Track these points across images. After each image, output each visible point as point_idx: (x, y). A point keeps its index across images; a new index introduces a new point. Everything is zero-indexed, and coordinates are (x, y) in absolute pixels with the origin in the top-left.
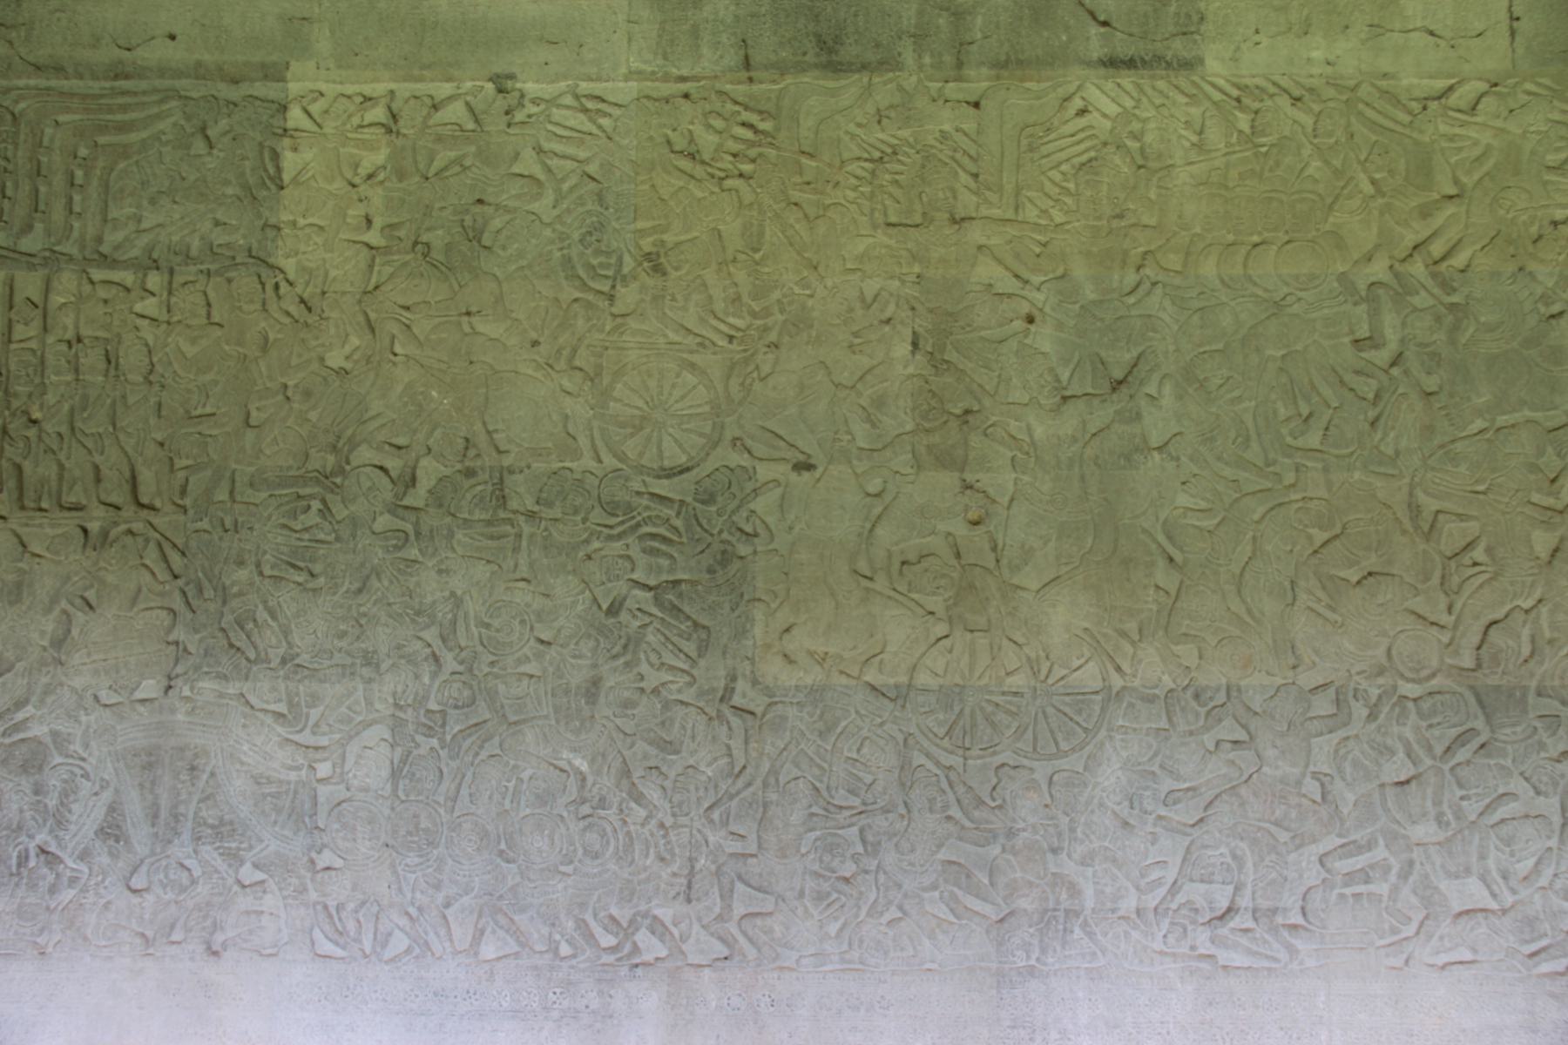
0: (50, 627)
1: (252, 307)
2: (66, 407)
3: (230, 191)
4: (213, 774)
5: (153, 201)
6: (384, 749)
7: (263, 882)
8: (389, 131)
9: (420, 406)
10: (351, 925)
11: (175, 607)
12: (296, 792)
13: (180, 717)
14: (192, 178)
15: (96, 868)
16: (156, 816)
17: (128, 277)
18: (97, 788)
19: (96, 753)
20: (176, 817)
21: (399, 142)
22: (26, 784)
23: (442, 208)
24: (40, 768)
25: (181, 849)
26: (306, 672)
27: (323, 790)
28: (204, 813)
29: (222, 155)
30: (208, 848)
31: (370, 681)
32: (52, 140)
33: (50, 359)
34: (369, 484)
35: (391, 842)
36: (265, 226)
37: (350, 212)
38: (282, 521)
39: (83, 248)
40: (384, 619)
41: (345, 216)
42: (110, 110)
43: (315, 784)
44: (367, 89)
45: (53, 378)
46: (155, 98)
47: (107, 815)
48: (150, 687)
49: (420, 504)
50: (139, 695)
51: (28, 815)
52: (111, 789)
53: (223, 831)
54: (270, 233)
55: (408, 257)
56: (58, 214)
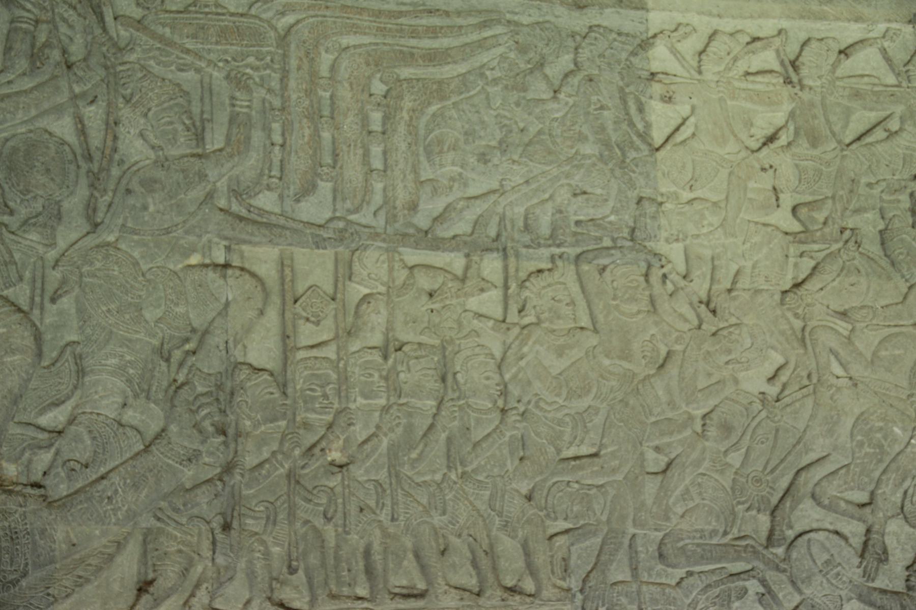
1: (634, 308)
3: (589, 149)
5: (483, 158)
8: (788, 81)
9: (881, 447)
14: (533, 130)
17: (457, 262)
21: (806, 96)
23: (870, 185)
29: (571, 101)
32: (333, 68)
33: (356, 373)
34: (826, 557)
36: (640, 200)
37: (752, 184)
39: (392, 219)
41: (746, 189)
42: (414, 33)
44: (752, 27)
45: (361, 401)
46: (472, 20)
49: (900, 586)
54: (650, 209)
55: (835, 247)
56: (353, 171)
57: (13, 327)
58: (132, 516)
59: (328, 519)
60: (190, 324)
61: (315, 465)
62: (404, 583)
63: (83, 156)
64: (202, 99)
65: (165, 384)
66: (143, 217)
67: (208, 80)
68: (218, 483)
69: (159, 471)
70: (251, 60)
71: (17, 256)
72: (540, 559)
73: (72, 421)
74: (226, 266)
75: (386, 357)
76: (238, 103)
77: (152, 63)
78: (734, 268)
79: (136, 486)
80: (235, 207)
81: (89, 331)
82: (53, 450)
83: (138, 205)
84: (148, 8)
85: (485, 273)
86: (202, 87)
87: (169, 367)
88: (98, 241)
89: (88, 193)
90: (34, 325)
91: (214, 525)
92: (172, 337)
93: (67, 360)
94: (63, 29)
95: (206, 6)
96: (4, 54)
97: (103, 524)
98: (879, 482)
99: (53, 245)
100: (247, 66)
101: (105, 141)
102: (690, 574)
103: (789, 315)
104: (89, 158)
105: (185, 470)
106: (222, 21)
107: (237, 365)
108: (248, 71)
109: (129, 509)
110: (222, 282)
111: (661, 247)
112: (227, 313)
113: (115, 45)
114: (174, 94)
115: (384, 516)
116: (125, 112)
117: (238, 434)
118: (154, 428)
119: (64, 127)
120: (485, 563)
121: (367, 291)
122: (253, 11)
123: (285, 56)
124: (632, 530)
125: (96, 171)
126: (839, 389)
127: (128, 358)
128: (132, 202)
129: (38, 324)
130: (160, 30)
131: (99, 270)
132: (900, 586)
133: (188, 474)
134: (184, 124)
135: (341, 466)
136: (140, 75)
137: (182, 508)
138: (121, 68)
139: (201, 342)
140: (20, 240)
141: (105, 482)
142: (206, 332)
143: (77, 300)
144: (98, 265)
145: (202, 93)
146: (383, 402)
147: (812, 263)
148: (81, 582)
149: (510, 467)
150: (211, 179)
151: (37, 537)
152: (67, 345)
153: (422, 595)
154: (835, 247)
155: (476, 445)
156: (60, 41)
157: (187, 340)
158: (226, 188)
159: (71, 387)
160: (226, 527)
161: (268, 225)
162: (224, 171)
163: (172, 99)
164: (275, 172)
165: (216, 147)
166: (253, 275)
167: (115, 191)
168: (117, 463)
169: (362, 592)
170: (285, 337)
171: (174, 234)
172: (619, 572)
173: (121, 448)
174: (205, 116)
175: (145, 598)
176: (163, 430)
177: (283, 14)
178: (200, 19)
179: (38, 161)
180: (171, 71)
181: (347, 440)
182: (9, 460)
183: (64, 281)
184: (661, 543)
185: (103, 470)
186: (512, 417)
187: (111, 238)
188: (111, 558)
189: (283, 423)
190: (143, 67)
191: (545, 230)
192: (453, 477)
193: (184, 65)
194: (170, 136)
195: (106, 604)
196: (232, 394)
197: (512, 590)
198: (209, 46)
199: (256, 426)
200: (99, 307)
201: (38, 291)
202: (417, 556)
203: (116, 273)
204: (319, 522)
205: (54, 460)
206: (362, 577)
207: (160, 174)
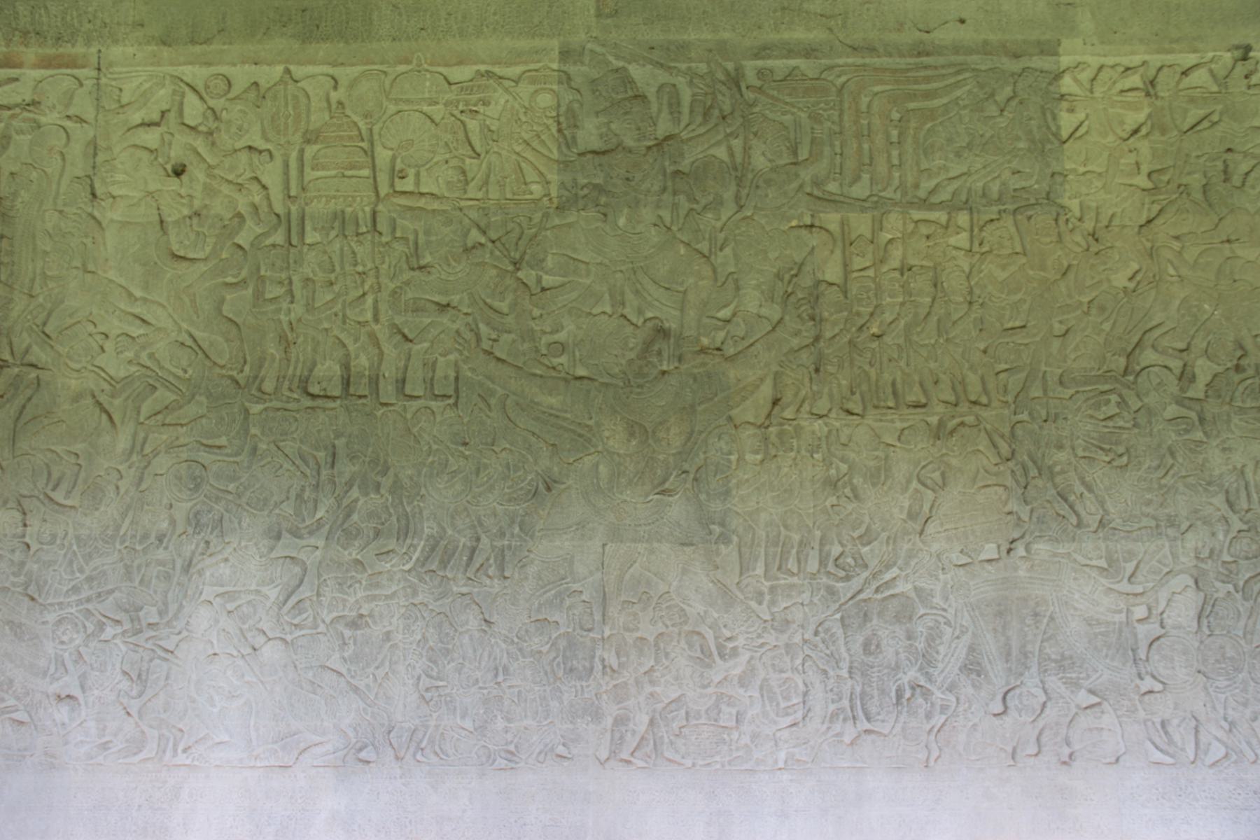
0: (907, 504)
1: (1048, 240)
2: (903, 322)
3: (1021, 145)
4: (1052, 618)
5: (958, 155)
6: (1191, 593)
7: (1099, 704)
8: (1148, 94)
10: (1177, 738)
11: (1008, 484)
12: (1120, 631)
13: (1021, 573)
14: (988, 135)
15: (962, 698)
16: (1009, 654)
17: (942, 216)
18: (957, 633)
19: (954, 604)
20: (1025, 655)
21: (1159, 103)
22: (900, 631)
23: (1198, 157)
24: (910, 618)
25: (1031, 682)
26: (1123, 534)
27: (1142, 629)
28: (1048, 651)
29: (1011, 116)
30: (1054, 678)
31: (1175, 539)
32: (869, 106)
35: (1203, 669)
36: (1053, 175)
37: (1122, 161)
38: (1090, 412)
39: (905, 193)
40: (1181, 488)
42: (916, 82)
43: (1136, 625)
44: (1126, 61)
46: (951, 70)
47: (968, 655)
48: (990, 551)
49: (1201, 395)
50: (983, 557)
51: (902, 656)
52: (970, 633)
53: (1064, 663)
56: (882, 168)
59: (871, 365)
61: (864, 336)
62: (914, 399)
70: (822, 105)
72: (991, 386)
73: (734, 315)
74: (812, 226)
75: (902, 274)
78: (1110, 212)
80: (816, 192)
85: (960, 223)
98: (1193, 337)
102: (1077, 392)
103: (1143, 240)
104: (736, 169)
107: (819, 282)
111: (1065, 201)
115: (902, 364)
116: (754, 142)
117: (821, 320)
118: (776, 317)
119: (721, 153)
120: (959, 388)
121: (890, 237)
123: (841, 101)
124: (1043, 368)
126: (1172, 283)
130: (771, 92)
132: (1201, 395)
133: (795, 342)
135: (878, 337)
139: (799, 270)
142: (802, 264)
146: (901, 300)
147: (1159, 207)
148: (744, 399)
149: (974, 334)
153: (924, 406)
154: (1174, 196)
155: (954, 323)
160: (817, 370)
161: (834, 201)
164: (838, 171)
166: (827, 231)
169: (891, 404)
170: (845, 265)
172: (1036, 392)
175: (777, 408)
177: (839, 76)
181: (881, 322)
183: (726, 240)
184: (1061, 375)
185: (752, 341)
186: (975, 306)
188: (758, 387)
189: (845, 314)
191: (995, 196)
192: (941, 341)
196: (818, 298)
197: (975, 403)
199: (831, 314)
202: (921, 385)
204: (867, 367)
206: (891, 397)
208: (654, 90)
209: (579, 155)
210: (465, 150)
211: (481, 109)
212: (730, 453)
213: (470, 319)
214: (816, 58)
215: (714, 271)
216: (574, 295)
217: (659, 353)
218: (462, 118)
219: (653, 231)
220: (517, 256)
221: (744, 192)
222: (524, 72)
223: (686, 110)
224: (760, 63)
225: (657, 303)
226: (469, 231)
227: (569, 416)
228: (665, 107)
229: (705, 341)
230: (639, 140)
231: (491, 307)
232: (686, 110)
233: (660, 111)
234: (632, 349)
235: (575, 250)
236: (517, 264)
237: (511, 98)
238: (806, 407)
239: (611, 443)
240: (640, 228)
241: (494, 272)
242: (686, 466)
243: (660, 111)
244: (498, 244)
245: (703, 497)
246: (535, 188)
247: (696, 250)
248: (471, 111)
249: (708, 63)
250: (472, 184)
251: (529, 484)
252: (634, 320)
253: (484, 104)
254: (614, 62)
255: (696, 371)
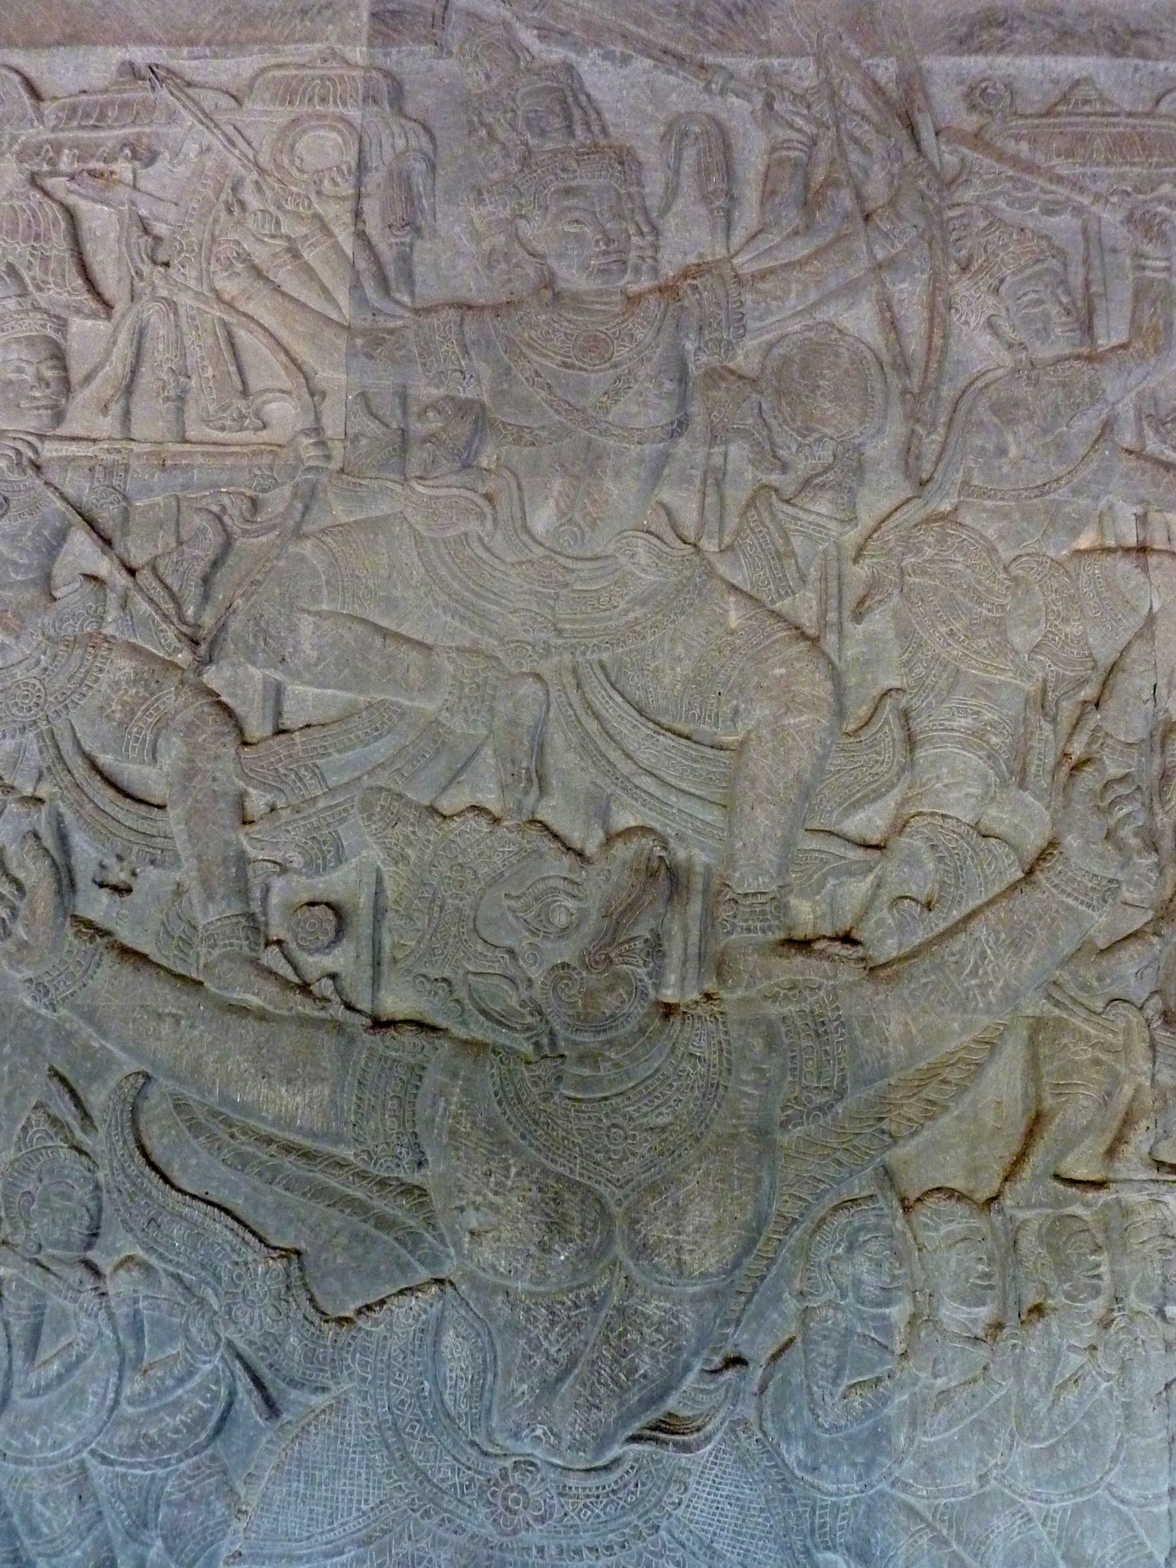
57: (797, 665)
58: (1011, 997)
60: (1091, 655)
63: (894, 365)
64: (1086, 261)
65: (1050, 760)
66: (1000, 468)
67: (1096, 227)
68: (1155, 940)
69: (1053, 919)
71: (797, 542)
73: (901, 826)
74: (1142, 549)
76: (1149, 263)
77: (1000, 203)
79: (1016, 946)
81: (920, 670)
82: (871, 877)
83: (990, 447)
84: (990, 112)
86: (1087, 239)
87: (1055, 731)
88: (922, 514)
89: (904, 430)
90: (830, 662)
91: (1149, 1012)
92: (1060, 678)
93: (887, 722)
94: (854, 156)
95: (1086, 102)
96: (762, 204)
97: (965, 1011)
99: (853, 520)
100: (1160, 200)
101: (930, 338)
105: (1095, 914)
106: (1114, 125)
108: (1162, 208)
109: (1007, 985)
110: (1142, 578)
112: (1153, 633)
113: (937, 176)
114: (1042, 251)
116: (962, 288)
118: (1034, 840)
119: (859, 320)
122: (1163, 107)
125: (916, 391)
127: (988, 716)
128: (980, 443)
129: (835, 658)
130: (1011, 147)
131: (931, 561)
133: (1100, 924)
134: (1061, 303)
136: (982, 223)
137: (1095, 984)
138: (951, 214)
140: (801, 514)
141: (963, 937)
142: (1113, 669)
143: (896, 615)
144: (929, 552)
145: (1087, 249)
150: (1111, 399)
151: (858, 1033)
152: (887, 693)
156: (850, 175)
157: (1082, 682)
158: (1131, 414)
159: (895, 769)
162: (1132, 381)
163: (1038, 261)
165: (1115, 341)
167: (949, 425)
168: (979, 902)
171: (1052, 496)
173: (986, 877)
174: (1093, 289)
176: (1052, 844)
178: (1077, 125)
179: (823, 377)
180: (1031, 214)
182: (803, 894)
183: (874, 585)
185: (956, 914)
187: (945, 507)
190: (987, 211)
193: (1055, 202)
194: (1039, 325)
195: (974, 1148)
198: (1095, 170)
200: (934, 626)
201: (833, 602)
203: (959, 566)
205: (875, 896)
207: (1023, 391)
208: (653, 131)
209: (416, 311)
210: (65, 291)
211: (123, 168)
212: (887, 1297)
213: (41, 818)
214: (1143, 54)
215: (835, 675)
216: (382, 749)
217: (656, 948)
218: (72, 200)
219: (641, 545)
220: (208, 620)
221: (931, 442)
222: (263, 71)
223: (751, 194)
224: (973, 64)
225: (646, 782)
226: (62, 535)
227: (347, 1153)
228: (689, 188)
229: (806, 914)
230: (604, 271)
231: (110, 782)
232: (751, 194)
233: (672, 191)
234: (564, 933)
235: (391, 604)
236: (204, 645)
237: (217, 145)
238: (1140, 1141)
239: (486, 1254)
240: (601, 542)
241: (126, 666)
242: (739, 1340)
243: (672, 191)
244: (145, 577)
245: (794, 1454)
246: (285, 414)
247: (777, 616)
248: (93, 174)
249: (820, 60)
250: (82, 396)
251: (204, 1387)
252: (576, 837)
253: (135, 156)
254: (536, 46)
255: (772, 1010)
